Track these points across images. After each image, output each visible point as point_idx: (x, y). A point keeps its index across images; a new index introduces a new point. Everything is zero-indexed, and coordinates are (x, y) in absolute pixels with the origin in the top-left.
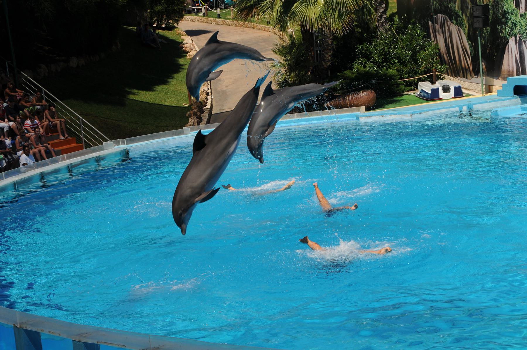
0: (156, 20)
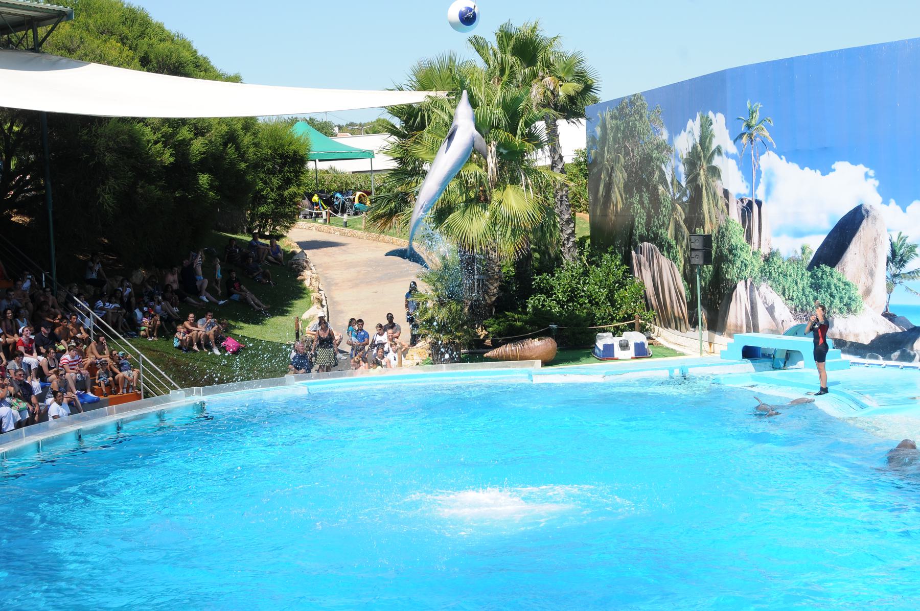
0: (258, 225)
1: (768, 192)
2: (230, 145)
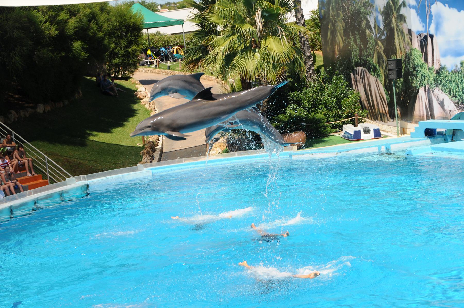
0: (114, 71)
1: (437, 28)
2: (93, 21)
